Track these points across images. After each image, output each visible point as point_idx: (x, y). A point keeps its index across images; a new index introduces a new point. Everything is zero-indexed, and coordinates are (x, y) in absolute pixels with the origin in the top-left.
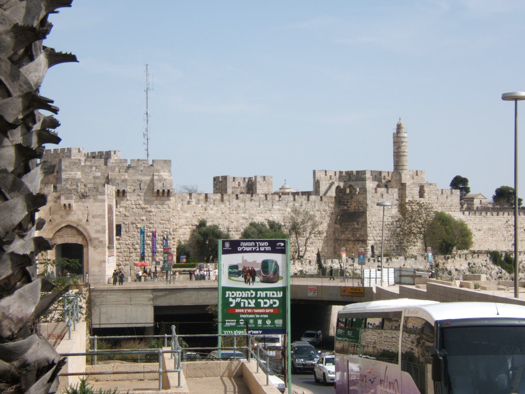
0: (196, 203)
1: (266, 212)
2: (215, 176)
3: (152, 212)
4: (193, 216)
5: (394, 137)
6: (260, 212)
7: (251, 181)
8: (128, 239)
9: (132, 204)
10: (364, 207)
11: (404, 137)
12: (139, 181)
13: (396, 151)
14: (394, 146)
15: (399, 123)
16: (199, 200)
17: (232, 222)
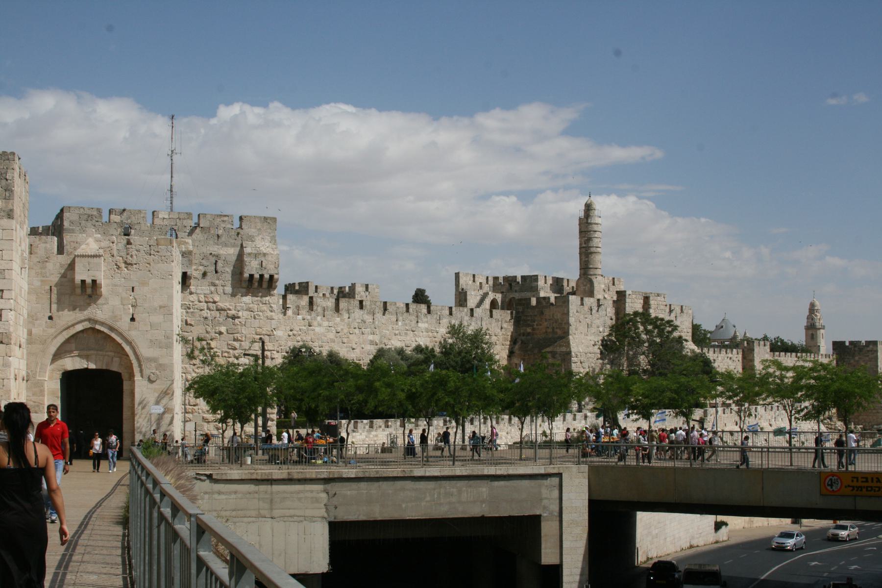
0: (294, 313)
1: (406, 334)
2: (287, 283)
3: (239, 317)
4: (289, 336)
5: (580, 224)
6: (397, 332)
7: (343, 292)
8: (191, 370)
9: (200, 302)
10: (564, 328)
11: (597, 224)
12: (214, 255)
13: (584, 245)
14: (581, 237)
15: (589, 202)
16: (298, 307)
17: (354, 349)
